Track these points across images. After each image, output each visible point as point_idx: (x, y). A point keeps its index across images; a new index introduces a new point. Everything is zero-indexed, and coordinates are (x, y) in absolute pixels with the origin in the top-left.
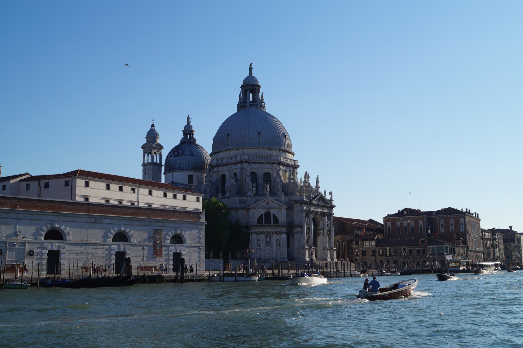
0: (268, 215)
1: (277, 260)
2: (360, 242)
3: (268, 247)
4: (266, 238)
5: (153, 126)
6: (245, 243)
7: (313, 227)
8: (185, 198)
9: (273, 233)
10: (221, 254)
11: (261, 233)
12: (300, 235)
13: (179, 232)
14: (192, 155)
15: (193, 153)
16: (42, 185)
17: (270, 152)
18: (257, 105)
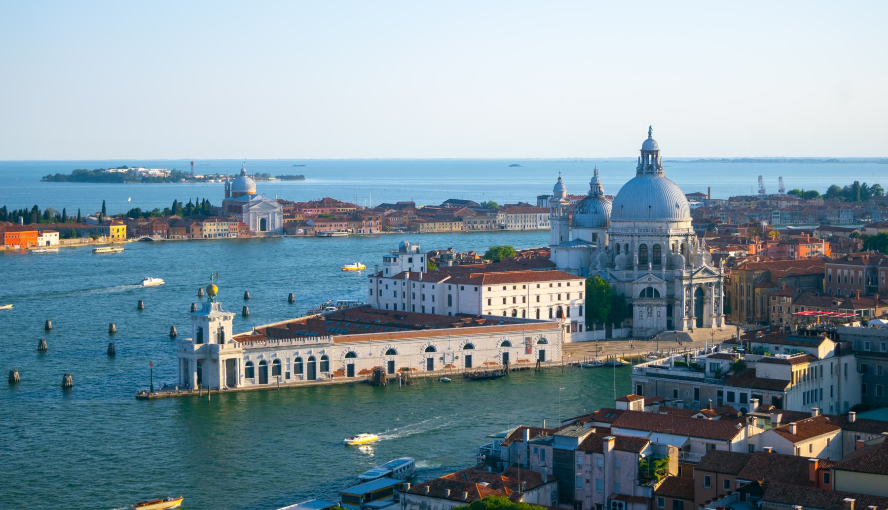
0: (650, 289)
1: (657, 329)
2: (777, 298)
3: (649, 318)
4: (648, 310)
5: (559, 178)
6: (630, 314)
7: (694, 298)
8: (568, 284)
9: (654, 305)
10: (604, 326)
11: (643, 306)
12: (679, 307)
13: (543, 337)
14: (596, 212)
15: (598, 211)
16: (460, 288)
17: (660, 225)
18: (653, 173)
